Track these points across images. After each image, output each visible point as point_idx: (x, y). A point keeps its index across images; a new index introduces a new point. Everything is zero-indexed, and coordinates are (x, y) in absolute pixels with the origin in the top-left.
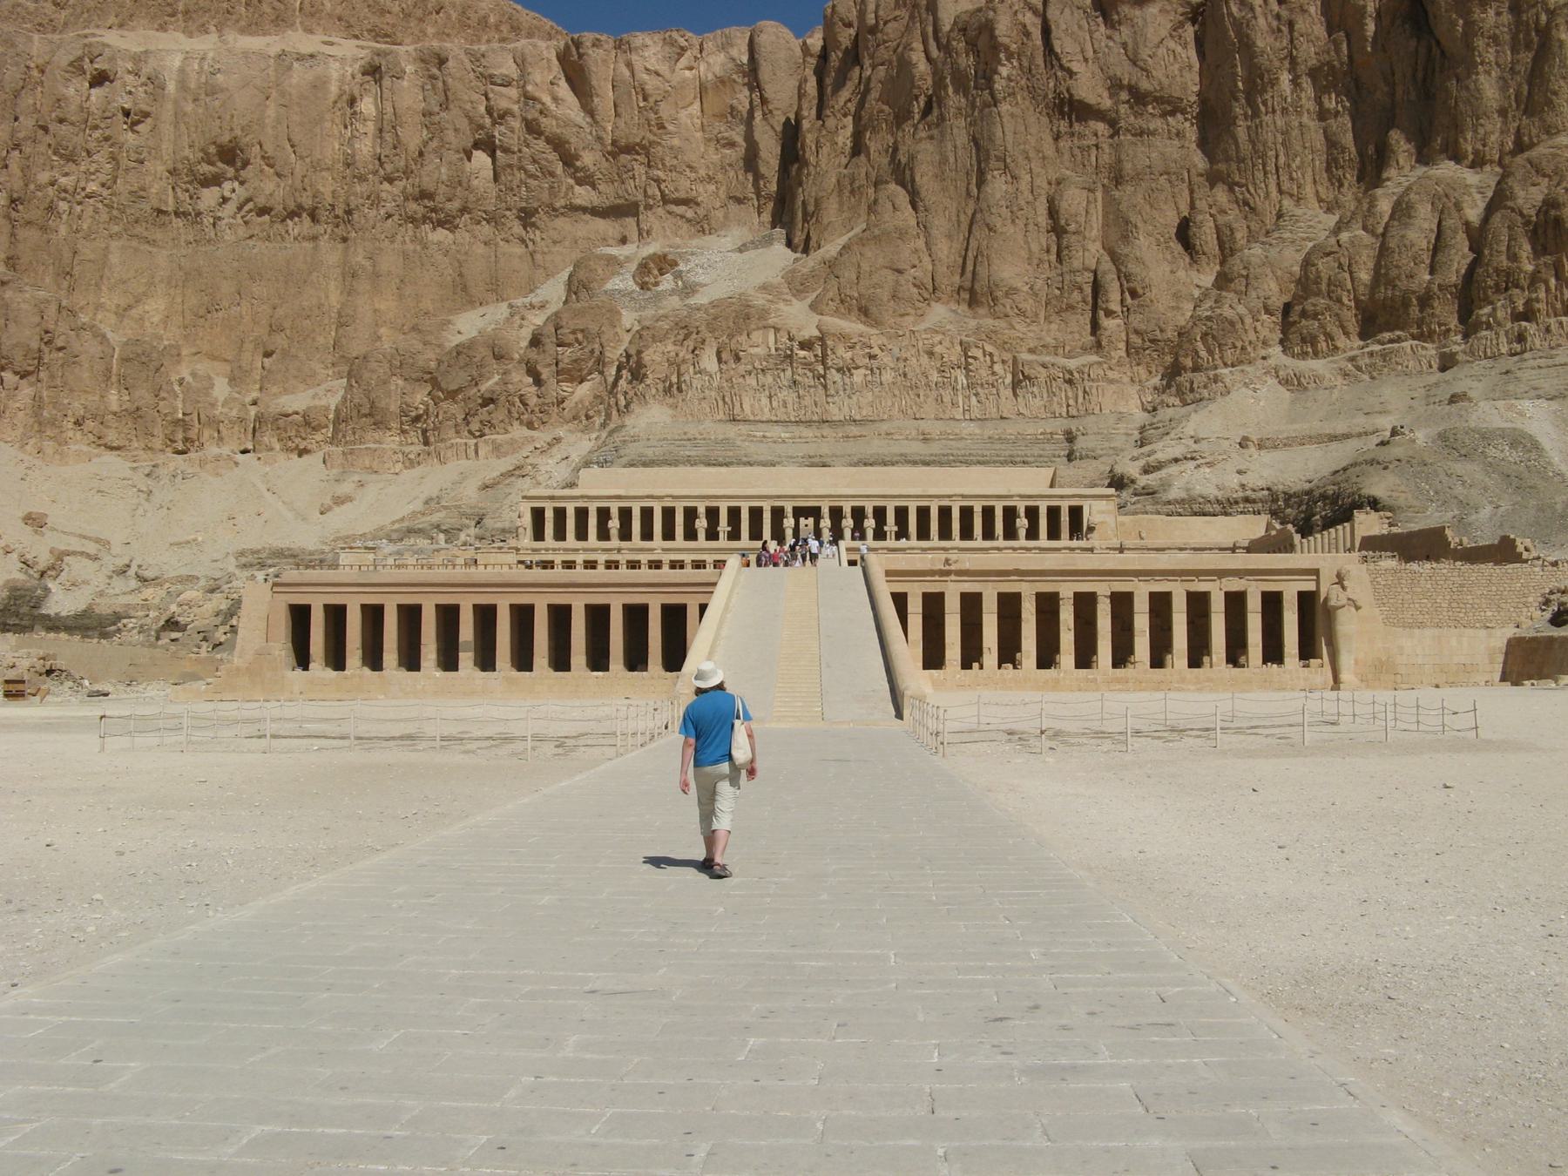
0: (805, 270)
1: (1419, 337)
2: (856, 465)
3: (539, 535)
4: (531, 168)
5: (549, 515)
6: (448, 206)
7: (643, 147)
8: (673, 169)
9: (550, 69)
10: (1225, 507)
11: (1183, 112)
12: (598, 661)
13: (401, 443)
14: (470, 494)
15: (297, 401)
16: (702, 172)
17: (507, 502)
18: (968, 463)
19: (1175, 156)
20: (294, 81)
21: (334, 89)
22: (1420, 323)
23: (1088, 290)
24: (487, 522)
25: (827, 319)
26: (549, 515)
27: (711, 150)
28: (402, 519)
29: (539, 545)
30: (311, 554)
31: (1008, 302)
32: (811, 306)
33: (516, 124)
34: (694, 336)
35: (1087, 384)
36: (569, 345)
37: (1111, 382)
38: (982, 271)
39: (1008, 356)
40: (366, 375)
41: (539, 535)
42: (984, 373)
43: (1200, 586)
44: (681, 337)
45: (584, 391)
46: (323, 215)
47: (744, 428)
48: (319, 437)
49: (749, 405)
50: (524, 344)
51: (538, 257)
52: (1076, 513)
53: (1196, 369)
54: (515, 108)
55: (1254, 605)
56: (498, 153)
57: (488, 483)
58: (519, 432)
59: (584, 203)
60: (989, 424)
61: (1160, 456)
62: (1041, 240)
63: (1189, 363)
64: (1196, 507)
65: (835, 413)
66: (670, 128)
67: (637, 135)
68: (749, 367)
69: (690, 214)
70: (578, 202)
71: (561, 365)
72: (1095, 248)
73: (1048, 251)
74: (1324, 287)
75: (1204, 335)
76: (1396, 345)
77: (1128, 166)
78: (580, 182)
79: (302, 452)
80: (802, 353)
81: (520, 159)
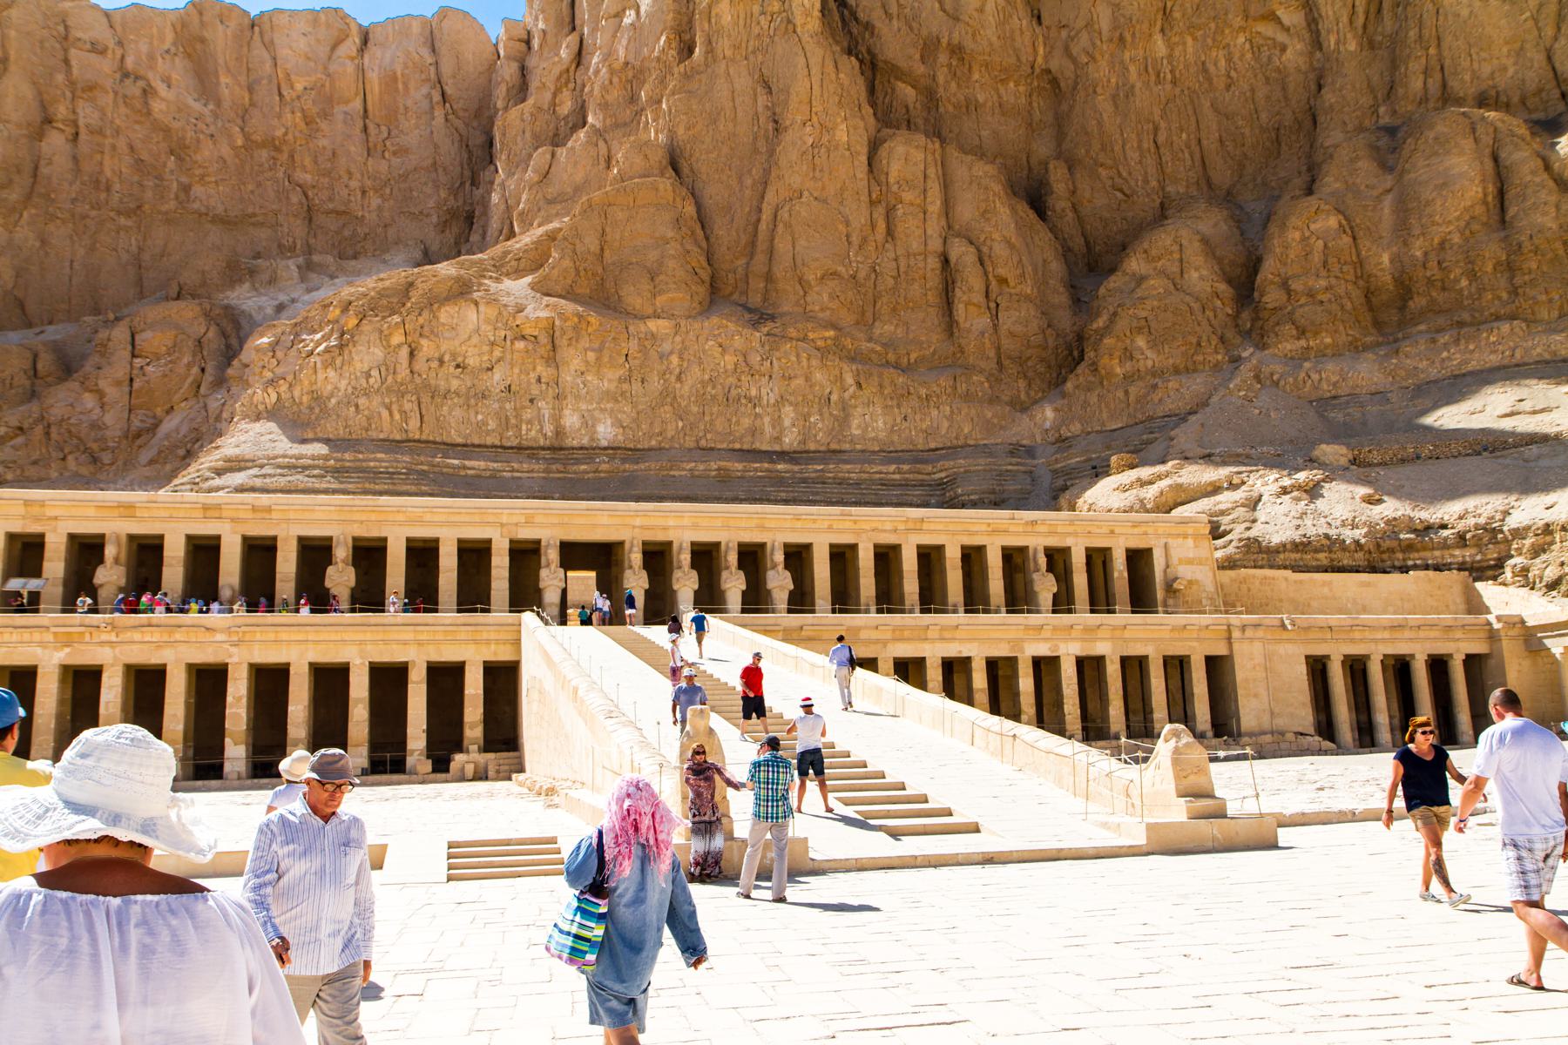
8: (327, 173)
23: (934, 281)
32: (533, 286)
33: (107, 100)
38: (782, 246)
52: (1138, 559)
54: (108, 84)
56: (83, 136)
66: (324, 125)
69: (347, 233)
70: (196, 206)
71: (136, 385)
73: (873, 227)
80: (520, 345)
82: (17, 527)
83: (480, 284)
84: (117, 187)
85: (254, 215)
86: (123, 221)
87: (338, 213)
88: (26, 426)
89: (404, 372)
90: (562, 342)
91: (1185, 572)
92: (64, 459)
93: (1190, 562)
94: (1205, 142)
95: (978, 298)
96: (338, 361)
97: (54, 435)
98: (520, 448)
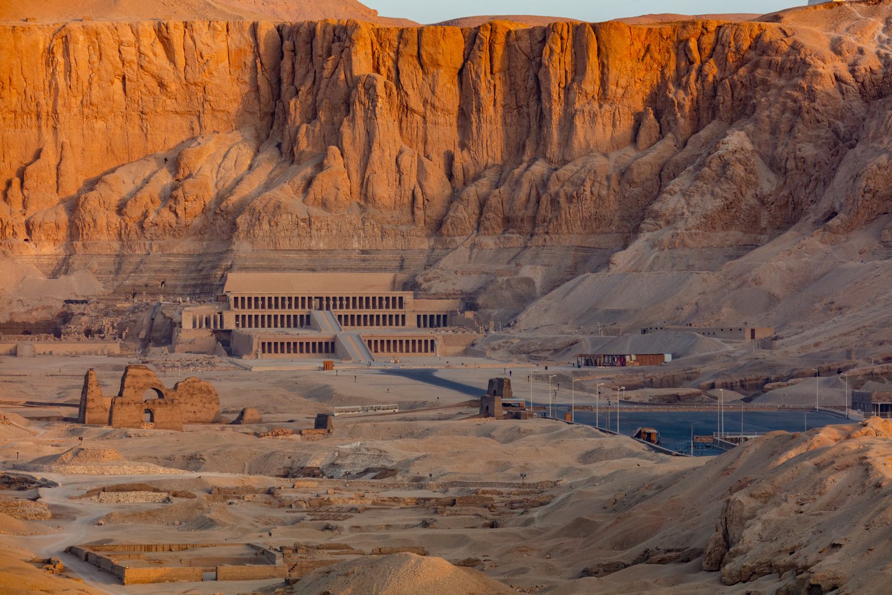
1: (519, 233)
4: (143, 90)
6: (104, 110)
7: (202, 83)
9: (151, 37)
10: (447, 296)
12: (308, 351)
16: (231, 97)
20: (23, 44)
21: (41, 46)
22: (520, 228)
25: (310, 208)
27: (235, 85)
33: (135, 67)
38: (370, 189)
39: (379, 226)
40: (89, 207)
42: (370, 231)
46: (44, 116)
49: (285, 244)
51: (149, 137)
52: (401, 298)
53: (448, 236)
62: (394, 176)
66: (215, 74)
67: (199, 78)
70: (169, 108)
72: (414, 180)
75: (451, 223)
77: (429, 138)
95: (421, 206)
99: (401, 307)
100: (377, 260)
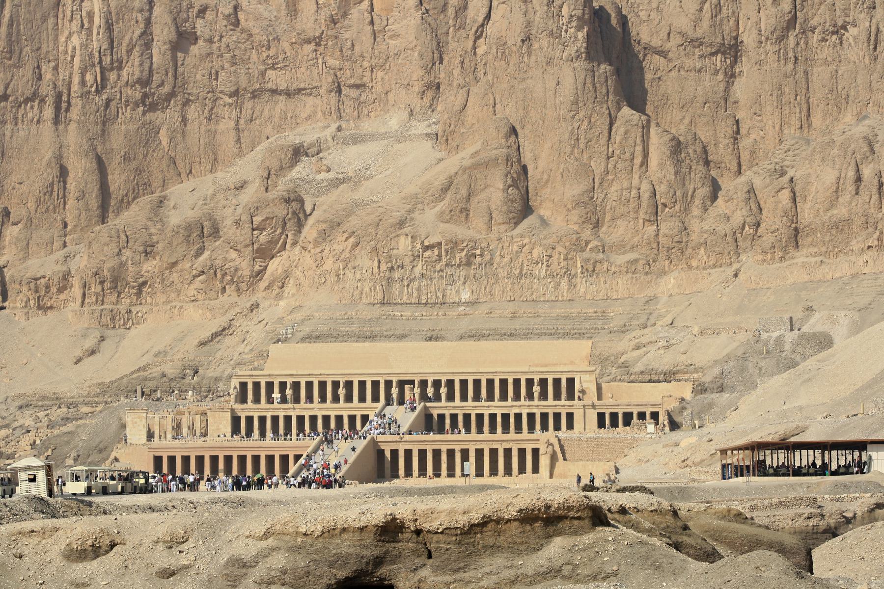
0: (437, 183)
2: (461, 338)
3: (243, 399)
5: (250, 387)
10: (668, 376)
11: (724, 53)
13: (132, 304)
14: (188, 350)
15: (45, 265)
16: (374, 61)
17: (218, 355)
18: (539, 335)
19: (716, 88)
23: (634, 204)
24: (201, 372)
25: (447, 225)
26: (250, 387)
28: (138, 370)
29: (244, 406)
30: (73, 398)
31: (576, 212)
34: (352, 240)
35: (630, 275)
36: (264, 229)
37: (646, 274)
41: (243, 399)
43: (495, 447)
44: (344, 239)
45: (275, 266)
47: (388, 309)
48: (62, 297)
50: (229, 222)
52: (571, 382)
55: (515, 453)
56: (201, 43)
57: (203, 341)
58: (224, 299)
59: (274, 87)
60: (558, 304)
61: (644, 340)
63: (694, 263)
64: (647, 378)
65: (451, 296)
68: (389, 265)
70: (269, 86)
71: (256, 246)
74: (779, 212)
76: (813, 260)
78: (273, 67)
79: (51, 308)
80: (427, 254)
81: (219, 48)
82: (268, 380)
83: (412, 219)
84: (222, 76)
85: (305, 89)
86: (227, 100)
87: (357, 86)
88: (205, 271)
89: (376, 270)
90: (443, 253)
91: (585, 386)
92: (225, 288)
93: (587, 382)
94: (811, 100)
96: (350, 265)
97: (219, 276)
98: (426, 304)
99: (571, 396)
100: (566, 317)
